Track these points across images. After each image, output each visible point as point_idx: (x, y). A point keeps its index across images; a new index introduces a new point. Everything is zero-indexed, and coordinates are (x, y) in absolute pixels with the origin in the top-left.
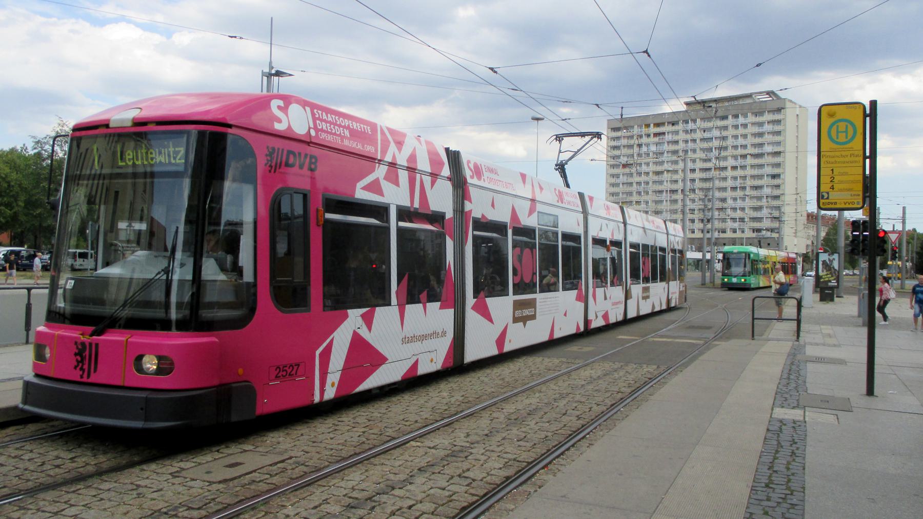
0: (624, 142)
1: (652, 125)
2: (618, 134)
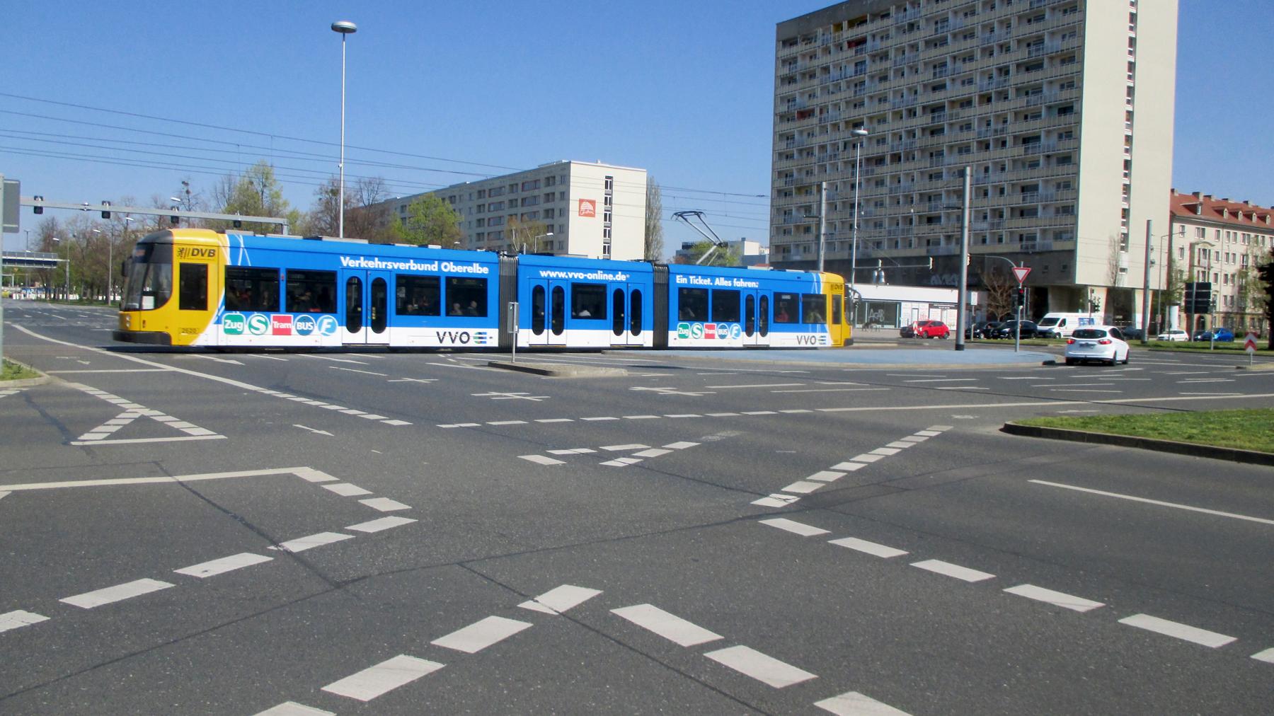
0: (802, 64)
1: (845, 24)
2: (794, 50)
